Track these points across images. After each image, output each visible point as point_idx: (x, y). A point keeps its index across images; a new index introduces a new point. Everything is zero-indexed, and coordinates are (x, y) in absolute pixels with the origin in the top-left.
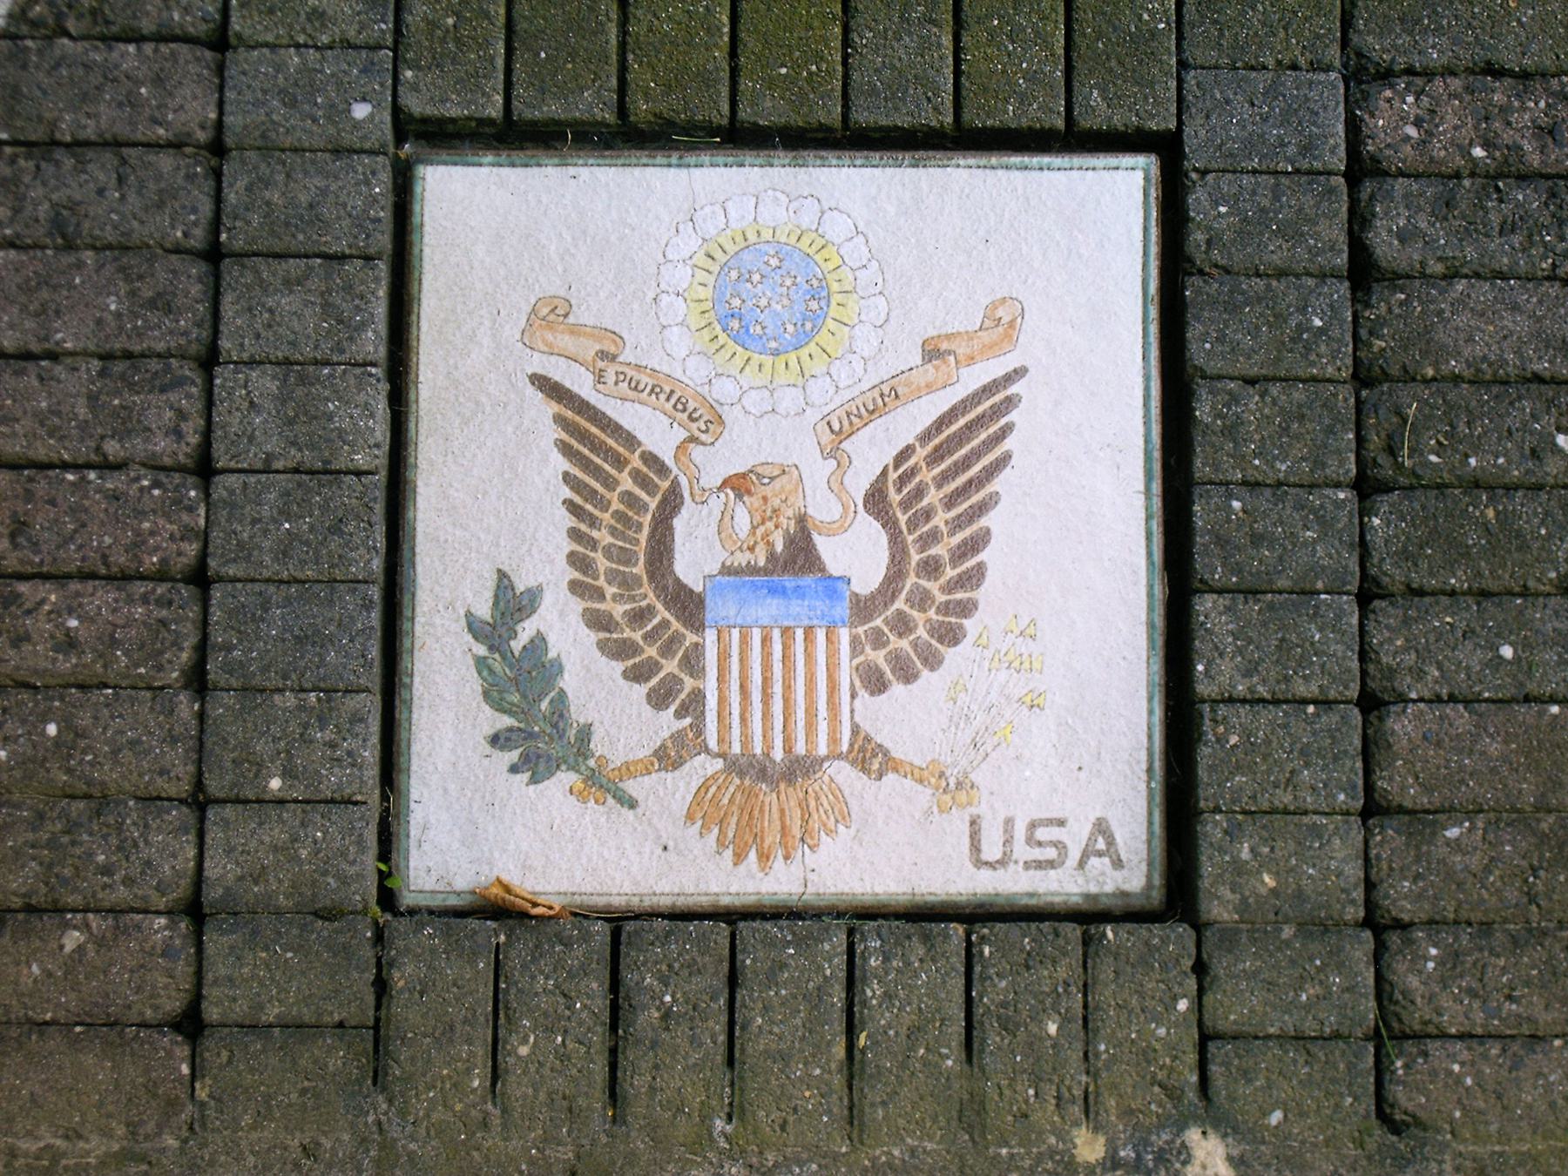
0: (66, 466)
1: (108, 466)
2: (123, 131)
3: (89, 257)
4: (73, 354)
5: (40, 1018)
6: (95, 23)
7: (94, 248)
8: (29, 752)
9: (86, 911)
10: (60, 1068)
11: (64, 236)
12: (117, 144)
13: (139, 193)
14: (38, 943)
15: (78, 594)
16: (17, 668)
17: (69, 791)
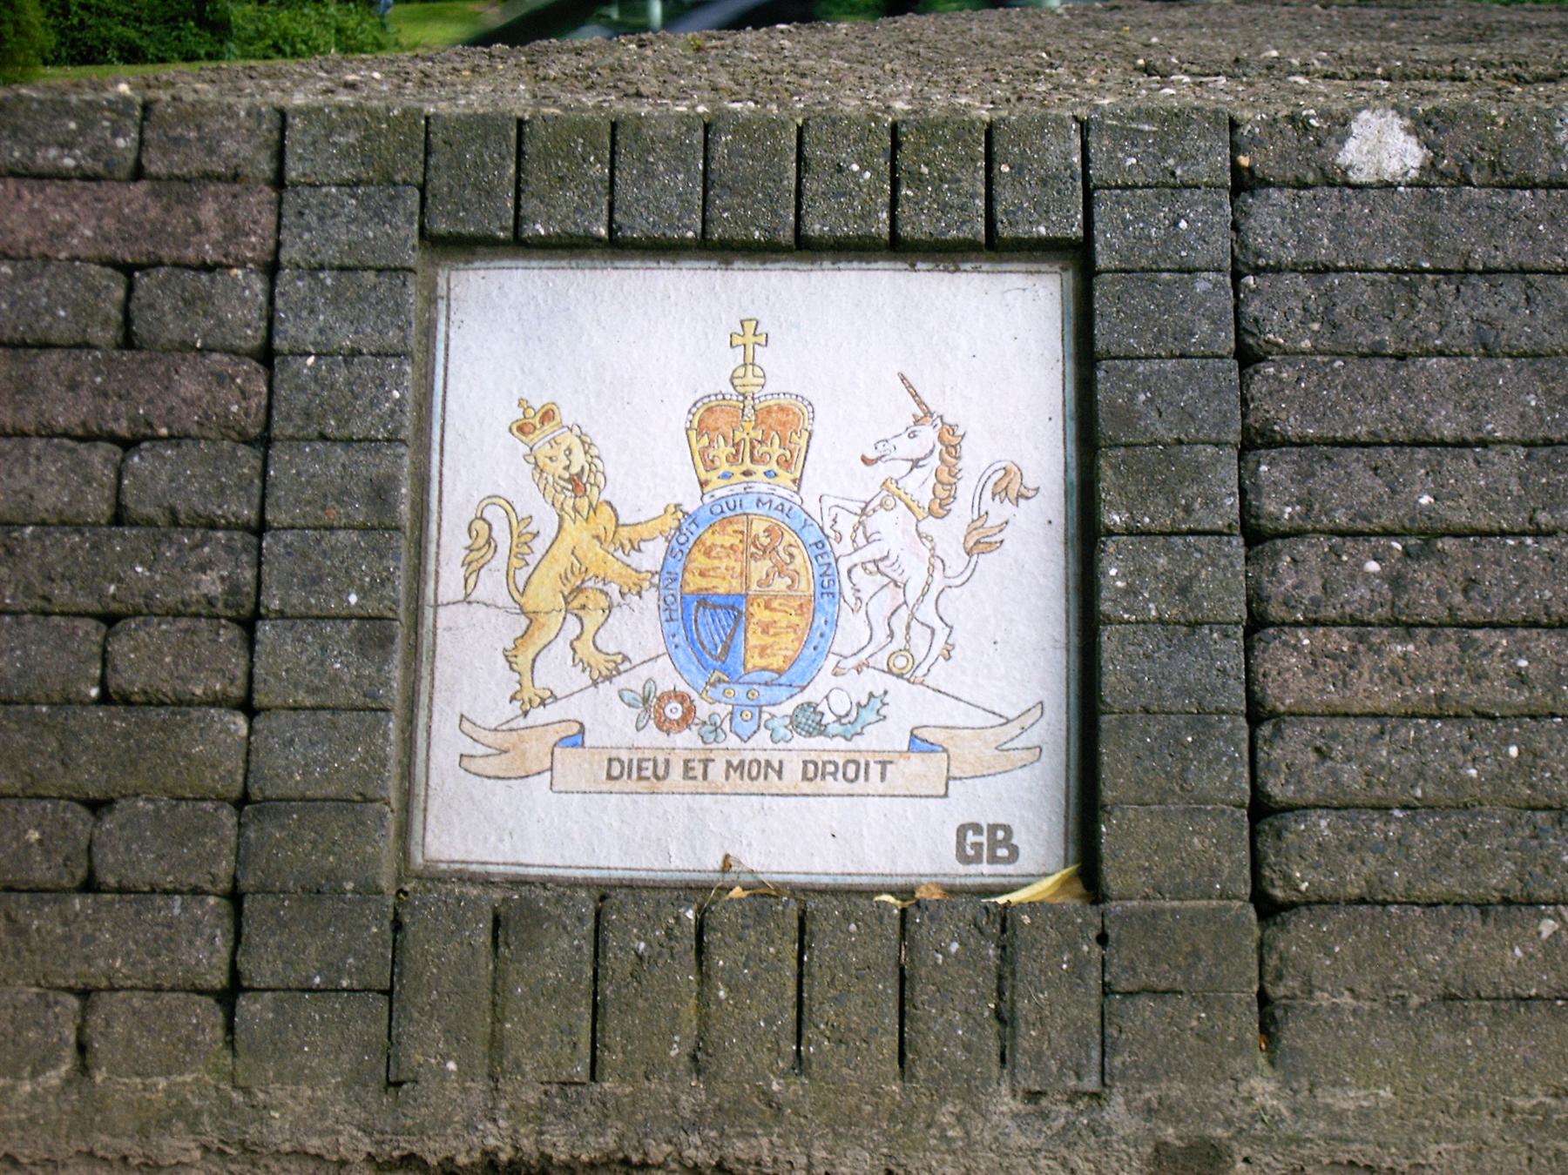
0: (1503, 534)
1: (1539, 533)
2: (1528, 260)
3: (1507, 363)
4: (1500, 442)
5: (1525, 995)
6: (1494, 173)
7: (1510, 356)
8: (1497, 770)
9: (1555, 904)
10: (1547, 1036)
11: (1485, 347)
12: (1522, 271)
13: (1546, 311)
14: (1519, 930)
15: (1525, 639)
16: (1479, 700)
17: (1532, 803)
